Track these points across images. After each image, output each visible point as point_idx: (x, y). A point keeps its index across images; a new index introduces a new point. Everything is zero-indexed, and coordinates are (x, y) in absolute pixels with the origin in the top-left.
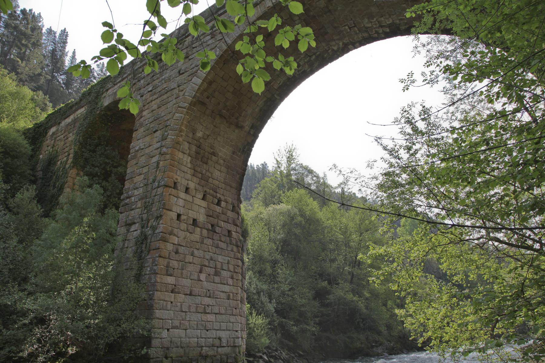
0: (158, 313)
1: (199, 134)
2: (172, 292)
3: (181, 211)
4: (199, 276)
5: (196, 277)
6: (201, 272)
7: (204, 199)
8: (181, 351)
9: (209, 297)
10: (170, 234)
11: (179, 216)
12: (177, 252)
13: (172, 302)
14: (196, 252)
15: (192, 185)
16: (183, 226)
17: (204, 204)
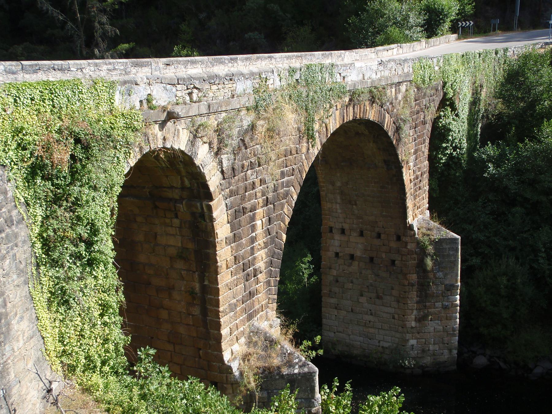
0: (324, 321)
1: (338, 184)
2: (336, 308)
7: (361, 234)
9: (371, 314)
11: (337, 254)
12: (337, 281)
13: (336, 316)
17: (361, 240)
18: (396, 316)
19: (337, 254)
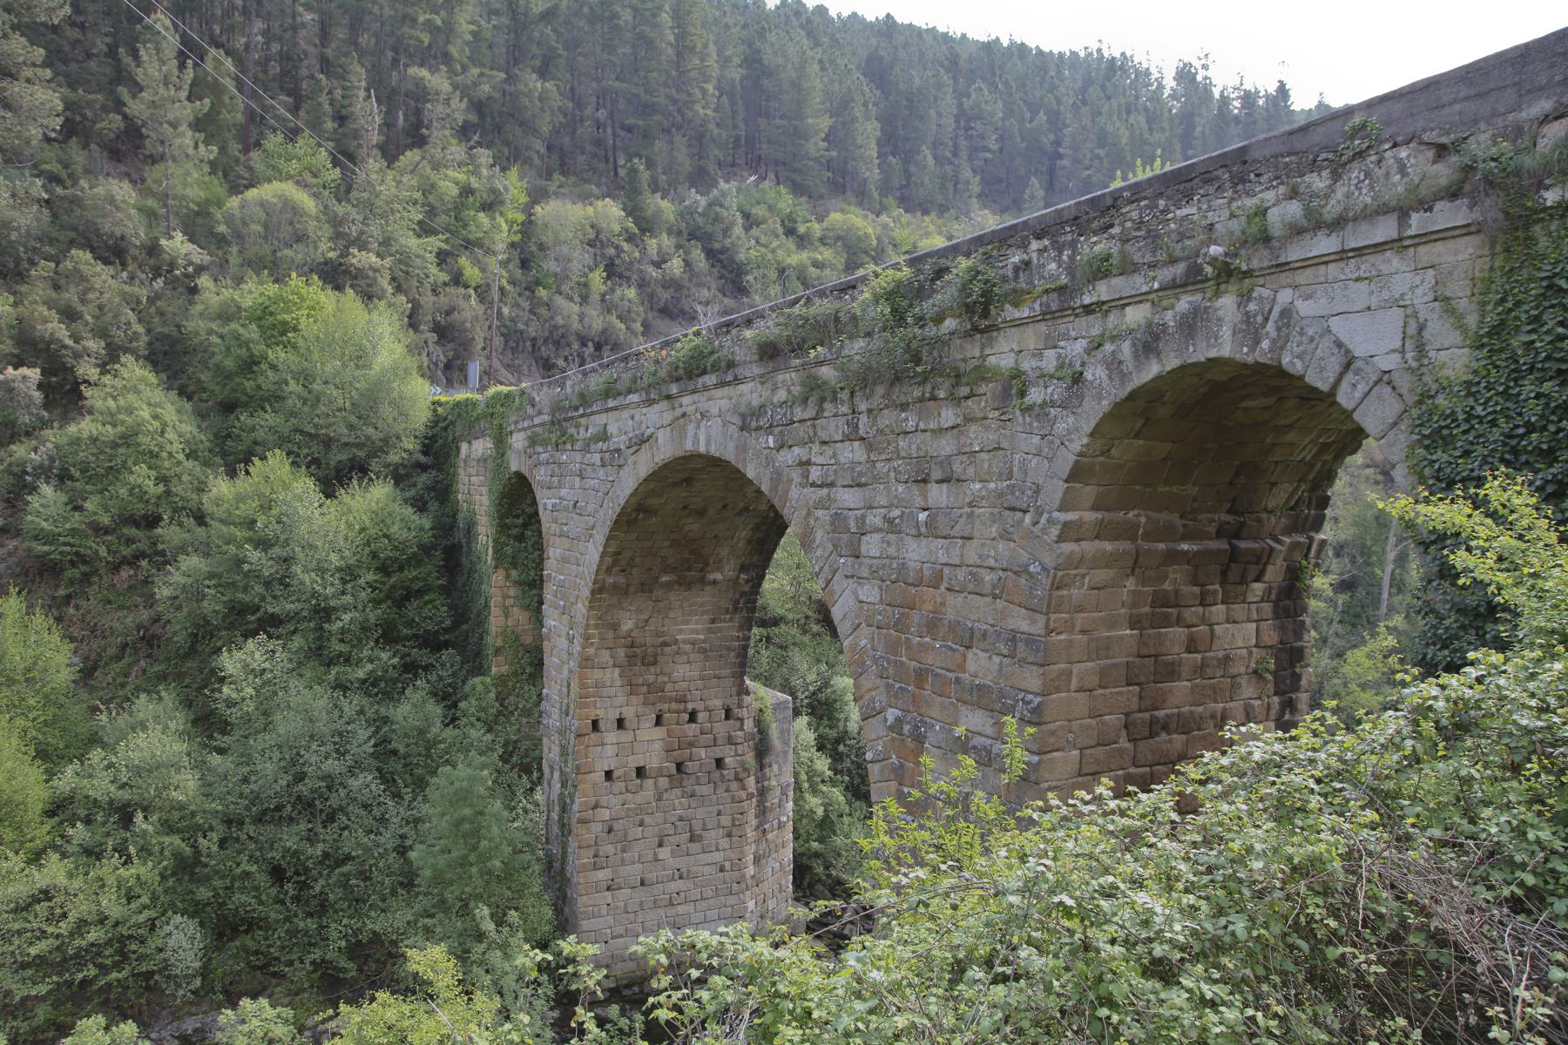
1: (627, 625)
2: (608, 889)
3: (611, 764)
4: (656, 855)
5: (650, 857)
6: (660, 845)
8: (632, 966)
9: (681, 878)
10: (595, 807)
11: (609, 775)
14: (648, 820)
15: (629, 713)
16: (619, 786)
17: (660, 732)
18: (727, 865)
19: (609, 775)
